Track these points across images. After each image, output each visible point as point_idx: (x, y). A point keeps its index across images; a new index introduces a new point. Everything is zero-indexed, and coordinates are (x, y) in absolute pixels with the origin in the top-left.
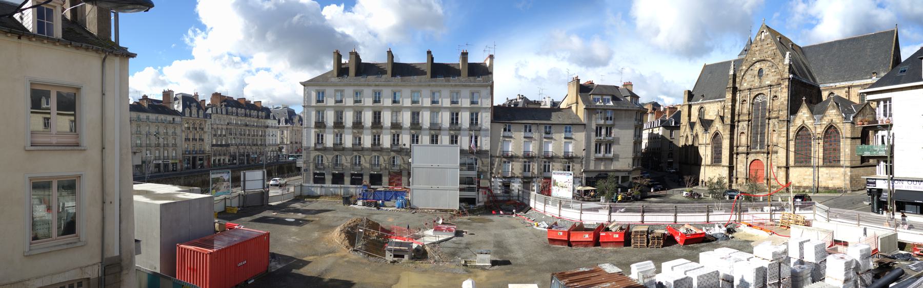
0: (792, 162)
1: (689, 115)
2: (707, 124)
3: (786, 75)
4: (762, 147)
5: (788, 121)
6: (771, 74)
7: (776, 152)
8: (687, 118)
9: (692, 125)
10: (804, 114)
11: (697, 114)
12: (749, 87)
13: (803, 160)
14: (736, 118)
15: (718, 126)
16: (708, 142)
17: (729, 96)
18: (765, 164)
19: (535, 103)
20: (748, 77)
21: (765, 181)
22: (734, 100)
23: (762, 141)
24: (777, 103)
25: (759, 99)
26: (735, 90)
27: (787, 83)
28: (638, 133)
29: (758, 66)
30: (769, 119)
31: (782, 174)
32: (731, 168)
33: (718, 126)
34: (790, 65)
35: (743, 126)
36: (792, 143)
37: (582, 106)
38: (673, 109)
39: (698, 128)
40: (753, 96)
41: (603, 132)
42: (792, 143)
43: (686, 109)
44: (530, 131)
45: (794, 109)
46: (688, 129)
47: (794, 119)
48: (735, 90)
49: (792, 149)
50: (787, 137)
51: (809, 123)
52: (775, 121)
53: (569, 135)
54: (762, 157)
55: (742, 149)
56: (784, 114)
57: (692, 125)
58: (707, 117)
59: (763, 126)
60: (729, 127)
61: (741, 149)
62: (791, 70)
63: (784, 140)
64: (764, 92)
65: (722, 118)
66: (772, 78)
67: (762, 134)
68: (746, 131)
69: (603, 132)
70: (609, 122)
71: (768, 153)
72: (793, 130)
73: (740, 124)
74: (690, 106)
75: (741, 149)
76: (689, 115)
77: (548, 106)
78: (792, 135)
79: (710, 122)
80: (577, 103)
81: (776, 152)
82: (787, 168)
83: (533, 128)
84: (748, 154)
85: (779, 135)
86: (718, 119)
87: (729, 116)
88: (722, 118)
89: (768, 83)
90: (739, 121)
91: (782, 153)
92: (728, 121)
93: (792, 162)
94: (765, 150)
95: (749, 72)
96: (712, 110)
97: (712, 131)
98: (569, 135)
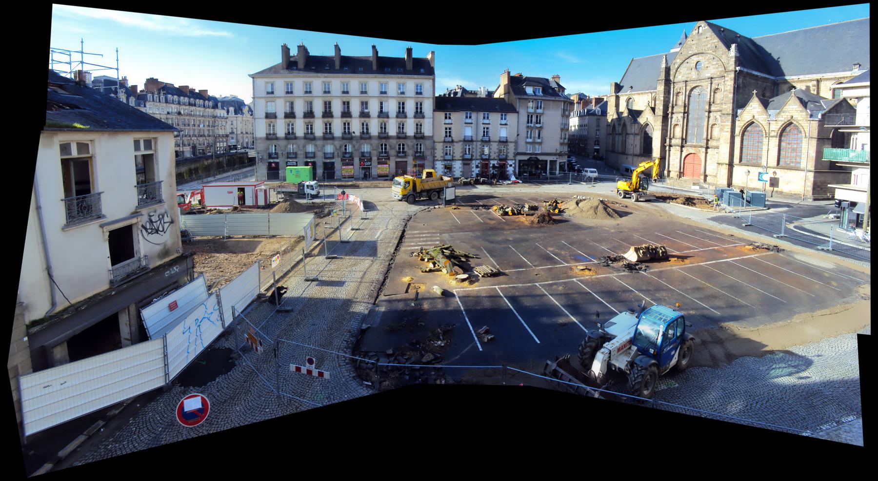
1: (617, 106)
3: (732, 65)
5: (734, 116)
6: (712, 67)
7: (717, 148)
8: (614, 108)
10: (754, 109)
11: (625, 104)
12: (684, 79)
14: (670, 110)
16: (636, 132)
17: (661, 88)
20: (683, 69)
21: (702, 177)
22: (667, 92)
23: (699, 135)
24: (719, 96)
25: (696, 92)
26: (668, 82)
27: (732, 75)
29: (695, 59)
30: (710, 112)
31: (724, 170)
34: (736, 57)
35: (677, 118)
38: (599, 101)
40: (689, 88)
41: (534, 119)
42: (738, 140)
45: (740, 103)
47: (741, 114)
48: (668, 82)
52: (718, 115)
55: (676, 141)
56: (728, 107)
58: (636, 107)
59: (700, 118)
60: (661, 118)
61: (673, 142)
62: (739, 61)
64: (703, 84)
66: (713, 71)
67: (699, 126)
69: (534, 119)
70: (539, 111)
72: (740, 125)
76: (617, 106)
78: (738, 130)
82: (731, 165)
84: (682, 147)
85: (721, 130)
87: (662, 108)
88: (653, 109)
89: (709, 75)
93: (736, 160)
94: (704, 143)
95: (685, 64)
98: (504, 122)
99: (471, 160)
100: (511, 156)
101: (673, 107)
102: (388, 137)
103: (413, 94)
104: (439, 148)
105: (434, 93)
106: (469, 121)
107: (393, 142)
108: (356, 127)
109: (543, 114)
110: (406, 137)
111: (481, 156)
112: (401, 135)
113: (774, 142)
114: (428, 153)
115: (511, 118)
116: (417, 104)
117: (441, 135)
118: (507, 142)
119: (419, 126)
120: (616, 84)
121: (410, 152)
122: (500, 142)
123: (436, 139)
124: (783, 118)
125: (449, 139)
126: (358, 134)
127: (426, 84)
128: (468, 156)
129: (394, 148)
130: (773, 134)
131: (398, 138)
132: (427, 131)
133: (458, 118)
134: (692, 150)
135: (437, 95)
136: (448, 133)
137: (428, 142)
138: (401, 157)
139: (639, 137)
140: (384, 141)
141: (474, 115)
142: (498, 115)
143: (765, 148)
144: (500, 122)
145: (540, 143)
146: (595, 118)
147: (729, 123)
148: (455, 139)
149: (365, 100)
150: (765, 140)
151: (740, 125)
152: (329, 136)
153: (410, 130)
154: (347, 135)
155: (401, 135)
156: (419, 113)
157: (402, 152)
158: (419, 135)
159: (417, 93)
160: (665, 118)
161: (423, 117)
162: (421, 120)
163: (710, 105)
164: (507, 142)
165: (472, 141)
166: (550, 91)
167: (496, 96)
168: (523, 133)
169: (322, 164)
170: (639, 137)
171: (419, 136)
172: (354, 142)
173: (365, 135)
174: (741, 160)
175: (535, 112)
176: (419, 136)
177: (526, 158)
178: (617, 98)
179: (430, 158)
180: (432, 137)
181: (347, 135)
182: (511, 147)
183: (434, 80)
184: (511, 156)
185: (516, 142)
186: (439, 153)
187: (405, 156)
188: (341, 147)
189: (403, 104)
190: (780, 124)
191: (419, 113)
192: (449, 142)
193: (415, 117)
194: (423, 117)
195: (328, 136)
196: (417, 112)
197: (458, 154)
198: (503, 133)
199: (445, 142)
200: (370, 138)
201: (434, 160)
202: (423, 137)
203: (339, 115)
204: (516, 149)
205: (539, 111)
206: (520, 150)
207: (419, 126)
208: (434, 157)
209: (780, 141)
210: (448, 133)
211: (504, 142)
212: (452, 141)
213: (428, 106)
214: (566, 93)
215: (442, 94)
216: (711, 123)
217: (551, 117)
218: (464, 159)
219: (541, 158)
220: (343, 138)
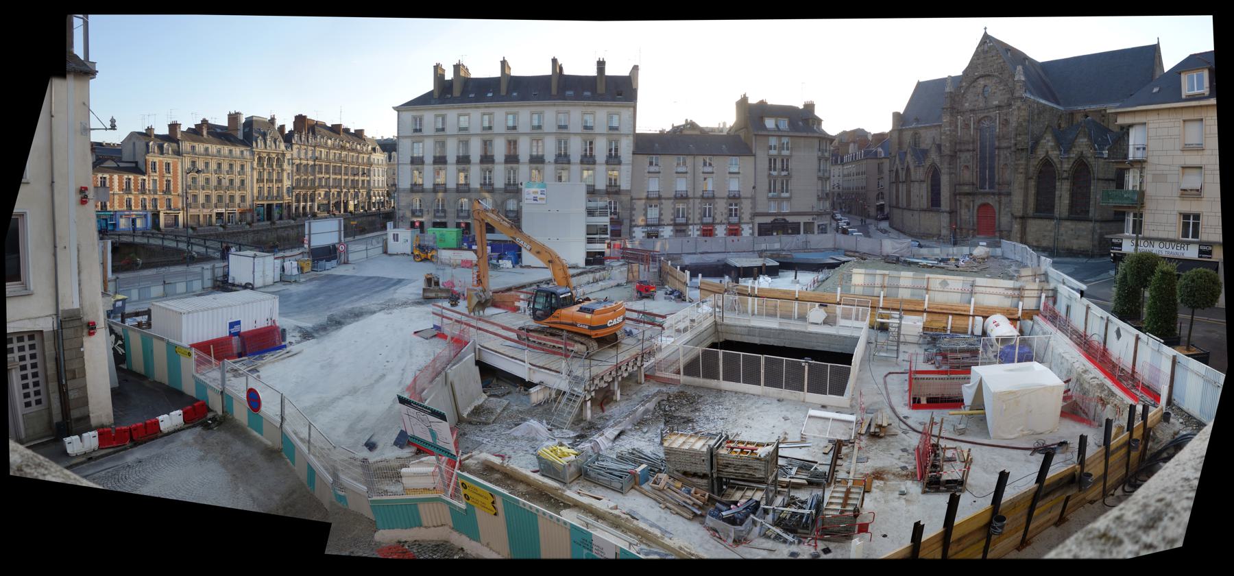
0: (1031, 211)
2: (921, 154)
15: (934, 156)
16: (922, 178)
33: (934, 156)
36: (1032, 183)
41: (779, 165)
49: (1032, 191)
50: (1027, 173)
51: (1054, 154)
63: (1021, 178)
65: (939, 147)
67: (992, 169)
72: (1034, 162)
75: (966, 189)
79: (925, 153)
81: (1009, 194)
86: (933, 149)
91: (1017, 198)
92: (946, 151)
100: (746, 217)
109: (791, 156)
130: (1065, 175)
133: (668, 163)
139: (924, 185)
141: (689, 160)
147: (1023, 162)
148: (664, 196)
158: (614, 189)
164: (739, 198)
165: (687, 198)
166: (802, 121)
170: (924, 185)
174: (1037, 210)
177: (769, 220)
179: (626, 222)
184: (746, 217)
185: (753, 198)
190: (1072, 161)
194: (620, 163)
202: (618, 192)
204: (754, 206)
209: (1073, 184)
219: (790, 219)
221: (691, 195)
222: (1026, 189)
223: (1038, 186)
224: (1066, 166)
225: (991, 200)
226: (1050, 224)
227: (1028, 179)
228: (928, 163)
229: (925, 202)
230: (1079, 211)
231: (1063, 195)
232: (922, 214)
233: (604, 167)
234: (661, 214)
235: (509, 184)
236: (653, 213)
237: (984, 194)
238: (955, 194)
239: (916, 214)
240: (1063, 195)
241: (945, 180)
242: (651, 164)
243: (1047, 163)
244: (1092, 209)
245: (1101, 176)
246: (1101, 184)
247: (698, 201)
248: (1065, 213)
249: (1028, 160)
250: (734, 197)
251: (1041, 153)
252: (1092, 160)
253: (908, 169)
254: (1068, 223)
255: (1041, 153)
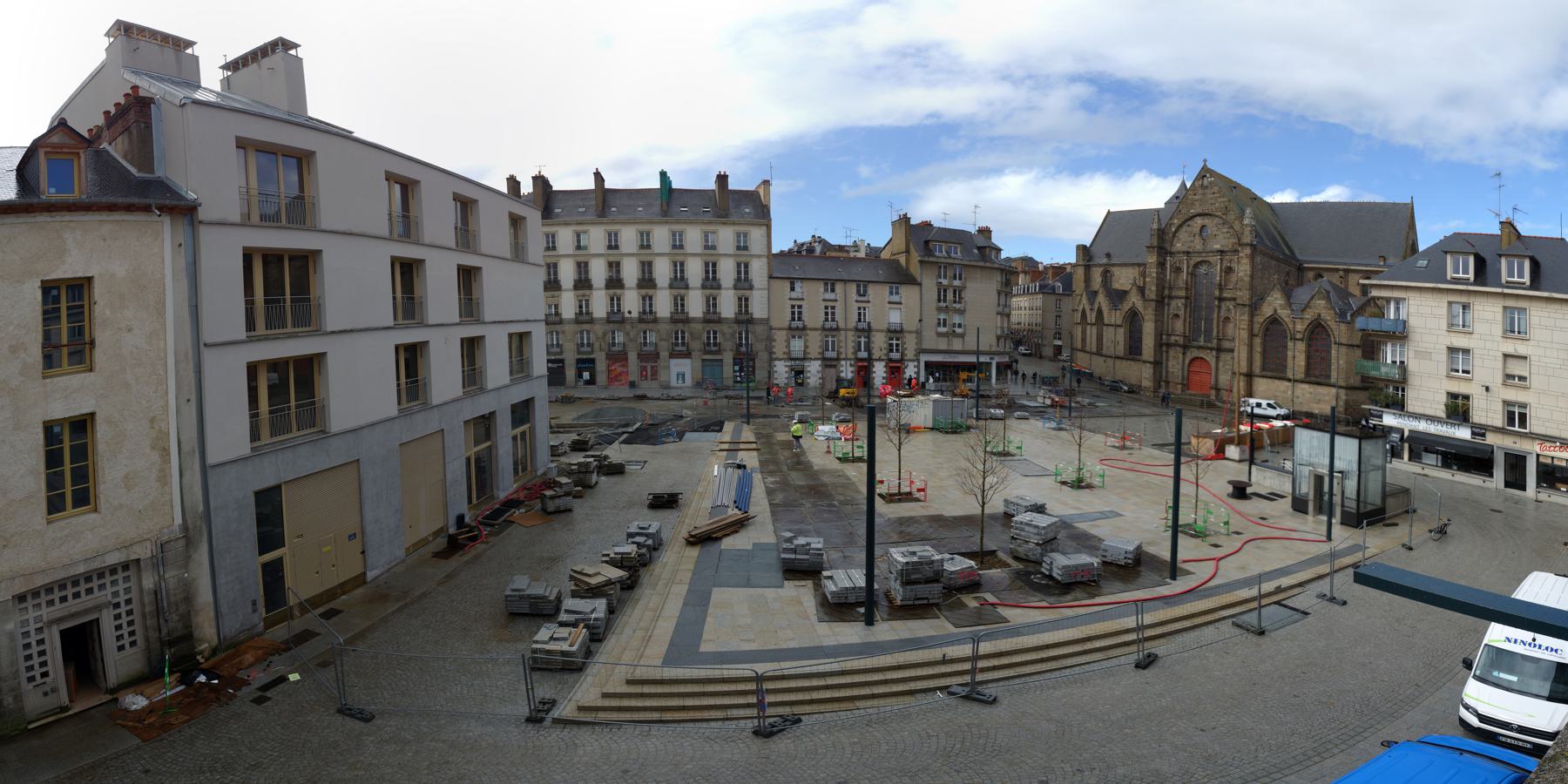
0: (1257, 370)
1: (1087, 280)
2: (1118, 297)
4: (1208, 338)
8: (1082, 285)
9: (1093, 295)
13: (1275, 369)
15: (1134, 299)
16: (1119, 322)
17: (1152, 259)
18: (1213, 364)
19: (841, 248)
21: (1213, 392)
22: (1161, 265)
23: (1208, 332)
28: (1002, 301)
30: (1221, 299)
32: (1157, 364)
35: (1178, 305)
36: (1258, 341)
37: (916, 257)
38: (1058, 270)
39: (1102, 299)
40: (1192, 262)
41: (950, 296)
43: (1080, 272)
44: (833, 290)
46: (1084, 301)
49: (1258, 348)
52: (1231, 305)
53: (895, 298)
54: (1210, 357)
57: (1093, 295)
58: (1116, 286)
59: (1210, 308)
63: (1244, 334)
65: (1142, 290)
67: (1209, 321)
68: (1181, 313)
69: (950, 296)
70: (957, 283)
71: (1219, 350)
72: (1259, 319)
73: (1174, 303)
74: (1088, 268)
76: (1087, 280)
77: (862, 254)
78: (1256, 327)
80: (907, 251)
81: (1232, 351)
82: (1249, 376)
83: (839, 287)
84: (1185, 347)
86: (1134, 291)
90: (1170, 297)
96: (1124, 279)
97: (1126, 306)
98: (895, 298)
99: (838, 359)
101: (1170, 288)
102: (687, 320)
103: (731, 250)
104: (780, 337)
105: (769, 247)
106: (830, 296)
107: (700, 326)
108: (631, 303)
110: (720, 321)
111: (855, 353)
112: (712, 317)
113: (1301, 346)
114: (759, 347)
115: (908, 294)
116: (739, 265)
117: (783, 318)
118: (902, 331)
119: (743, 302)
120: (1084, 247)
121: (728, 345)
122: (889, 331)
123: (774, 323)
124: (1309, 316)
125: (800, 324)
126: (635, 314)
127: (756, 234)
128: (831, 354)
129: (699, 338)
130: (1299, 336)
131: (706, 321)
132: (758, 309)
134: (1196, 353)
135: (775, 250)
136: (797, 314)
137: (759, 329)
138: (711, 353)
139: (1121, 331)
140: (680, 326)
142: (886, 288)
143: (1290, 353)
144: (887, 298)
145: (962, 336)
146: (1053, 298)
147: (1246, 317)
149: (646, 259)
150: (1290, 344)
151: (1259, 319)
152: (585, 318)
153: (727, 306)
154: (616, 318)
155: (712, 317)
156: (743, 282)
157: (712, 348)
159: (738, 248)
160: (1161, 302)
161: (751, 288)
162: (747, 293)
163: (1221, 290)
164: (902, 331)
167: (885, 255)
168: (932, 316)
169: (573, 362)
170: (1121, 331)
171: (744, 319)
172: (628, 327)
173: (648, 317)
174: (1264, 368)
175: (950, 286)
176: (744, 319)
178: (1088, 268)
180: (765, 322)
181: (616, 318)
182: (910, 344)
183: (769, 227)
185: (918, 333)
186: (779, 349)
187: (718, 352)
188: (605, 334)
189: (714, 265)
191: (743, 282)
192: (797, 328)
193: (735, 287)
194: (751, 288)
195: (584, 316)
196: (739, 279)
197: (815, 350)
198: (895, 317)
199: (790, 328)
200: (656, 321)
201: (771, 360)
202: (751, 321)
203: (602, 284)
205: (957, 283)
206: (925, 346)
207: (743, 302)
208: (771, 353)
209: (1309, 346)
210: (797, 314)
211: (896, 333)
212: (804, 328)
213: (758, 270)
214: (1004, 255)
215: (786, 249)
216: (1223, 314)
217: (981, 292)
218: (824, 359)
220: (608, 321)
221: (841, 325)
222: (1251, 347)
223: (1264, 344)
224: (1299, 327)
225: (1210, 357)
226: (1283, 385)
227: (1252, 335)
228: (1126, 306)
229: (1121, 350)
230: (1316, 374)
231: (1297, 356)
232: (1118, 362)
233: (732, 292)
234: (806, 347)
235: (644, 312)
236: (797, 346)
237: (1200, 348)
238: (1162, 345)
239: (1110, 361)
240: (1297, 356)
241: (1148, 329)
242: (793, 289)
243: (1274, 321)
244: (1334, 374)
245: (1344, 341)
246: (1343, 350)
247: (850, 334)
248: (1301, 376)
249: (1252, 316)
250: (895, 331)
251: (1267, 311)
252: (1332, 324)
253: (1100, 312)
254: (1306, 386)
255: (1267, 311)
